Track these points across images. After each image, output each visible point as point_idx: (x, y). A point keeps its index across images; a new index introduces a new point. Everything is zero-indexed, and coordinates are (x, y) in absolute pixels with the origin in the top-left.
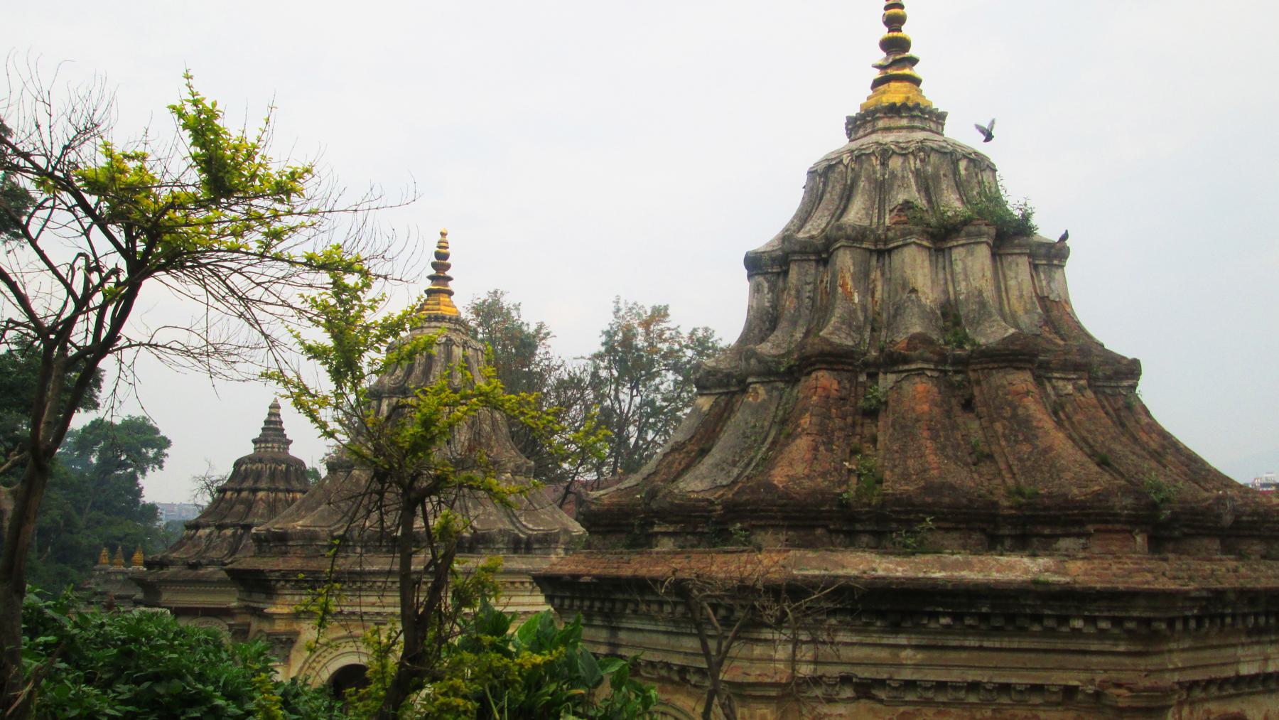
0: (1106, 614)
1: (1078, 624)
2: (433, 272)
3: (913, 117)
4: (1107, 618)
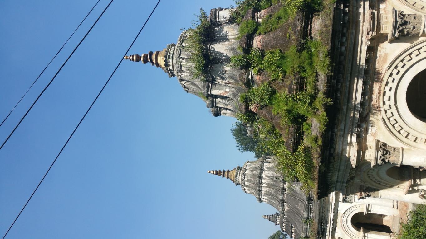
0: (340, 40)
1: (343, 48)
2: (221, 176)
3: (169, 58)
4: (342, 39)
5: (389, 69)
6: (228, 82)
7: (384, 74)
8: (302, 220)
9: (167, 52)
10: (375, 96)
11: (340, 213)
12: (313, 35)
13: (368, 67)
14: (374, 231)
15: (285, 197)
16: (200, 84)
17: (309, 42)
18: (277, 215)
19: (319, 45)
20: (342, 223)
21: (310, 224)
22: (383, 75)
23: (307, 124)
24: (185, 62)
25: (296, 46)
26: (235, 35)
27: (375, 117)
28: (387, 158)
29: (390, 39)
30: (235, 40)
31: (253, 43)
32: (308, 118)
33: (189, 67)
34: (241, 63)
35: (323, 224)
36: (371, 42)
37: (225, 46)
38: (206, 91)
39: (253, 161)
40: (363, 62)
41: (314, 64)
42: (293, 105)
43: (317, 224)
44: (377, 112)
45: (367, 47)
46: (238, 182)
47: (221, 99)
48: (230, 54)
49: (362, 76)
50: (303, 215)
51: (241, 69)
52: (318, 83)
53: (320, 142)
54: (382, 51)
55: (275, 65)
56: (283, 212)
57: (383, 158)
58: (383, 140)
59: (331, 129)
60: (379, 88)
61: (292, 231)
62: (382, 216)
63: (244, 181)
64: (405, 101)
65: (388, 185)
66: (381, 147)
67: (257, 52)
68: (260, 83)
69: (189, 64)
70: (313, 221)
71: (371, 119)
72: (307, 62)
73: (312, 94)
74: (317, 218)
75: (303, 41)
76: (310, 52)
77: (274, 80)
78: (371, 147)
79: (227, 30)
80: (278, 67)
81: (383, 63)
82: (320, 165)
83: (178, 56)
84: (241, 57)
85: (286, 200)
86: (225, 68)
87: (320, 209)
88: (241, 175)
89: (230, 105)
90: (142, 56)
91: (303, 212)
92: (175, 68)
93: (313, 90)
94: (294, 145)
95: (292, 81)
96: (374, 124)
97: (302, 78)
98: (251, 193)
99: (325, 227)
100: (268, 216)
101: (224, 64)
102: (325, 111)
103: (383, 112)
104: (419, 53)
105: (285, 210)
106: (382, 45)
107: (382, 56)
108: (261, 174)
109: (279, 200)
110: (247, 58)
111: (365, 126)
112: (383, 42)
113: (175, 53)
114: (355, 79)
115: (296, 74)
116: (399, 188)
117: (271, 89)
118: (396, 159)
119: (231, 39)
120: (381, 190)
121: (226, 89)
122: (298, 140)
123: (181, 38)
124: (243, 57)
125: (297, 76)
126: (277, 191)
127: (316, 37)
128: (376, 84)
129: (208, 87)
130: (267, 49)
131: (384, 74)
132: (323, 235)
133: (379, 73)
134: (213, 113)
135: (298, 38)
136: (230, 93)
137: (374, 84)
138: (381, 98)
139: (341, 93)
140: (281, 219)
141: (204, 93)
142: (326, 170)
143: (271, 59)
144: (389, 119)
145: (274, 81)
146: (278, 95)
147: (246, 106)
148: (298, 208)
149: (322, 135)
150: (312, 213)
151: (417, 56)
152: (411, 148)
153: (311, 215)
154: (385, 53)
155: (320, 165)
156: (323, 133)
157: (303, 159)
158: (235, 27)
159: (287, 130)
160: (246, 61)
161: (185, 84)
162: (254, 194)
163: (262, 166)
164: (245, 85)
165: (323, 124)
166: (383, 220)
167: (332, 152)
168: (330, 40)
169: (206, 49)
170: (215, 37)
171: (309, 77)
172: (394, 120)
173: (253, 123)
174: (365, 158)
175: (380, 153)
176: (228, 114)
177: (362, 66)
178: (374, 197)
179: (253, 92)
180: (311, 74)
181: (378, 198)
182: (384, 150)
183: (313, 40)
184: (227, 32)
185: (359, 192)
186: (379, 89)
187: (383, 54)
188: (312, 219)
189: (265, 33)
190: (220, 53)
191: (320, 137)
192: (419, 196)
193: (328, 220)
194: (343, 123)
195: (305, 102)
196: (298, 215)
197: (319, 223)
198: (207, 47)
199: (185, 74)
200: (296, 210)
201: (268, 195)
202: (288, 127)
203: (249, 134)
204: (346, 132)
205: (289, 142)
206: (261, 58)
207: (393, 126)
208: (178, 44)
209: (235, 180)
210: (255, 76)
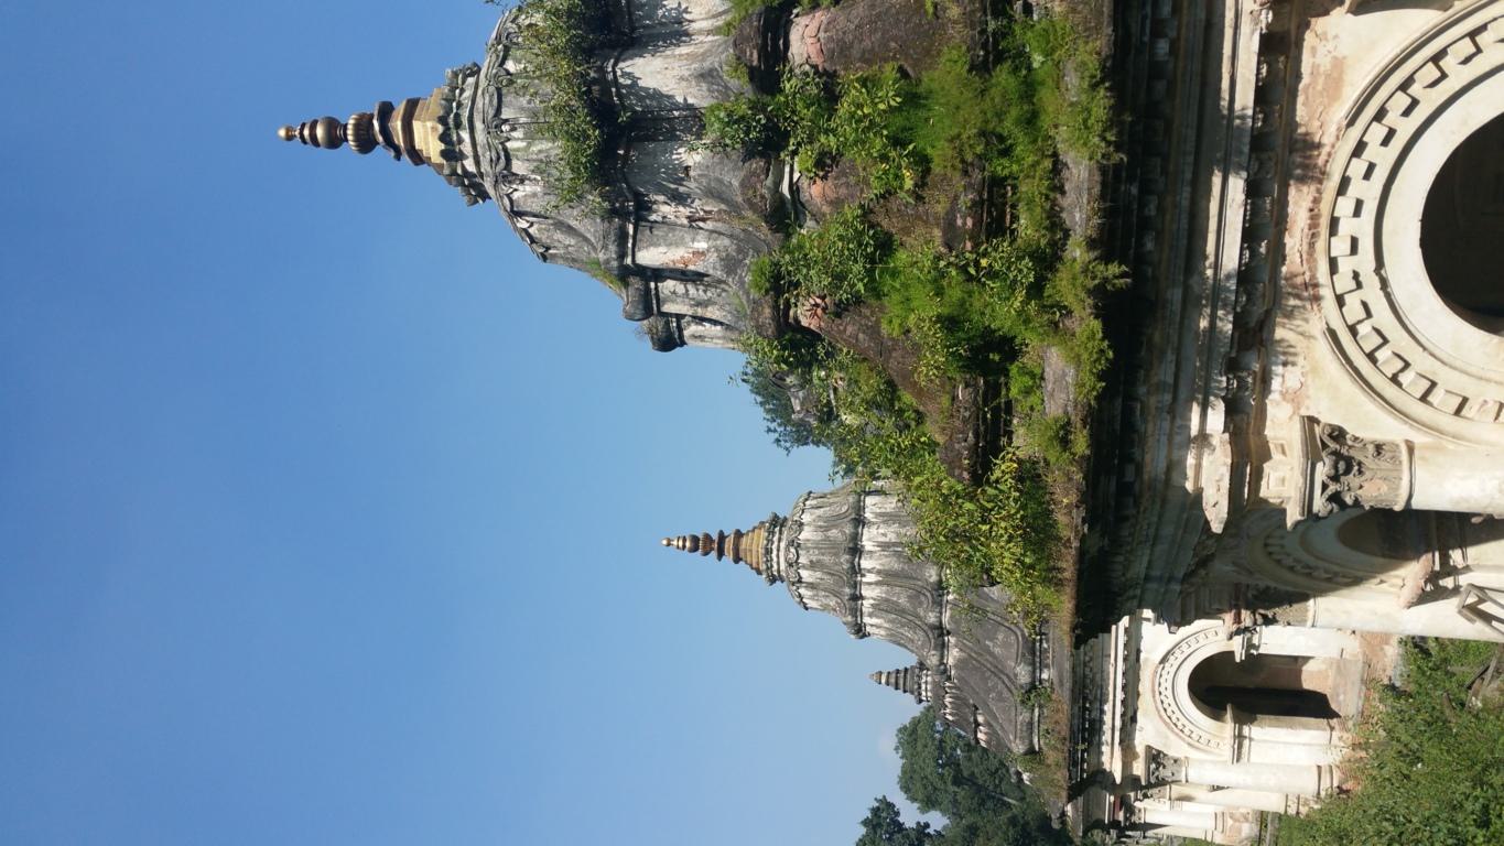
0: (1149, 9)
1: (1163, 47)
2: (714, 554)
3: (458, 125)
5: (1351, 123)
6: (702, 213)
7: (1333, 146)
8: (1011, 692)
9: (445, 100)
10: (1294, 242)
11: (1146, 659)
13: (1264, 121)
14: (1272, 717)
15: (948, 614)
16: (592, 228)
17: (1017, 29)
18: (921, 670)
19: (1063, 39)
20: (1157, 693)
21: (1040, 707)
22: (1325, 151)
23: (1025, 371)
24: (522, 139)
25: (964, 48)
26: (714, 17)
27: (1298, 326)
28: (1349, 490)
30: (716, 38)
31: (787, 45)
32: (1027, 345)
33: (536, 154)
34: (747, 134)
35: (1088, 705)
36: (1274, 15)
37: (676, 65)
38: (614, 256)
39: (826, 491)
40: (1245, 99)
41: (1045, 122)
42: (966, 296)
43: (1066, 707)
44: (1304, 307)
45: (1262, 36)
46: (775, 573)
47: (678, 283)
48: (698, 97)
49: (1244, 159)
50: (1016, 675)
51: (749, 155)
52: (1065, 202)
53: (1081, 444)
54: (1321, 50)
55: (885, 132)
56: (942, 667)
57: (1333, 488)
58: (1329, 416)
59: (1121, 388)
60: (1310, 205)
61: (976, 721)
62: (1296, 662)
63: (795, 568)
64: (1418, 251)
65: (1344, 577)
66: (1325, 446)
67: (808, 84)
68: (826, 209)
69: (539, 147)
70: (1054, 696)
71: (1279, 333)
72: (1014, 112)
73: (1039, 247)
74: (1068, 685)
75: (992, 25)
76: (1024, 72)
77: (883, 196)
78: (1282, 446)
80: (897, 142)
81: (1326, 100)
82: (1084, 535)
83: (490, 117)
84: (743, 109)
85: (953, 626)
86: (684, 157)
88: (783, 545)
89: (715, 303)
90: (351, 122)
91: (1013, 664)
92: (485, 167)
93: (1043, 232)
94: (978, 456)
95: (956, 198)
96: (1295, 354)
97: (996, 183)
98: (825, 608)
99: (1095, 714)
100: (889, 673)
101: (678, 138)
102: (1096, 317)
103: (1329, 302)
104: (1473, 50)
106: (1319, 24)
107: (1322, 69)
108: (856, 537)
109: (926, 628)
110: (769, 109)
111: (1256, 367)
112: (1326, 13)
113: (479, 103)
114: (1212, 174)
115: (970, 169)
116: (1384, 585)
117: (871, 232)
118: (1385, 488)
119: (700, 32)
120: (1315, 597)
121: (693, 240)
122: (991, 434)
123: (498, 40)
124: (750, 108)
125: (977, 176)
126: (916, 597)
127: (1049, 5)
128: (1301, 191)
129: (622, 237)
130: (846, 69)
131: (1333, 146)
132: (1090, 744)
133: (1310, 145)
134: (652, 338)
135: (973, 12)
136: (713, 257)
137: (1292, 191)
138: (1321, 245)
139: (1158, 239)
141: (607, 262)
142: (1107, 549)
143: (866, 111)
144: (1353, 330)
145: (882, 201)
146: (902, 257)
147: (776, 307)
148: (997, 650)
149: (1086, 417)
150: (1047, 666)
151: (1466, 61)
152: (1444, 443)
153: (1045, 676)
154: (1335, 58)
155: (1084, 535)
156: (1090, 404)
157: (1013, 512)
159: (945, 401)
160: (763, 122)
161: (531, 231)
162: (835, 610)
163: (859, 510)
164: (766, 222)
165: (1091, 371)
166: (1300, 671)
167: (1130, 475)
168: (1106, 15)
169: (601, 79)
170: (633, 29)
171: (1027, 177)
172: (1374, 332)
173: (810, 372)
174: (1263, 493)
175: (1322, 471)
176: (712, 338)
177: (1243, 118)
178: (1289, 624)
179: (800, 247)
180: (1034, 165)
181: (1304, 626)
182: (1336, 453)
183: (1035, 17)
184: (683, 7)
185: (1231, 611)
186: (1311, 210)
187: (1324, 62)
188: (1049, 689)
190: (657, 95)
191: (1079, 425)
192: (1460, 612)
193: (1107, 689)
194: (1170, 356)
195: (1015, 281)
196: (996, 675)
197: (1074, 700)
198: (602, 70)
199: (528, 188)
200: (990, 659)
201: (886, 611)
202: (948, 388)
203: (799, 412)
204: (1183, 394)
205: (957, 446)
206: (824, 105)
207: (1371, 357)
208: (487, 64)
209: (763, 567)
210: (804, 183)
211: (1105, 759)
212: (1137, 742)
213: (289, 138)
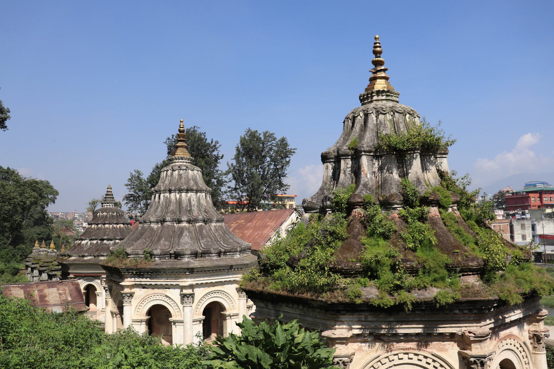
1: (457, 312)
3: (387, 96)
5: (432, 355)
10: (402, 345)
12: (462, 277)
29: (467, 354)
31: (433, 206)
34: (411, 196)
40: (441, 330)
43: (148, 267)
48: (412, 176)
50: (156, 249)
53: (358, 301)
57: (340, 362)
58: (355, 358)
71: (377, 344)
74: (157, 267)
79: (433, 170)
80: (421, 242)
87: (169, 269)
99: (146, 276)
103: (387, 355)
105: (152, 225)
106: (456, 345)
108: (192, 190)
112: (458, 346)
122: (346, 274)
123: (412, 110)
125: (419, 266)
126: (173, 212)
129: (370, 152)
133: (426, 346)
136: (366, 180)
137: (415, 343)
140: (111, 209)
141: (363, 147)
148: (162, 242)
150: (160, 260)
153: (156, 259)
158: (437, 181)
167: (342, 312)
169: (415, 149)
177: (436, 330)
187: (447, 347)
189: (443, 219)
190: (411, 165)
197: (151, 269)
198: (418, 149)
199: (375, 119)
210: (397, 211)
211: (129, 279)
212: (135, 289)
213: (376, 38)
